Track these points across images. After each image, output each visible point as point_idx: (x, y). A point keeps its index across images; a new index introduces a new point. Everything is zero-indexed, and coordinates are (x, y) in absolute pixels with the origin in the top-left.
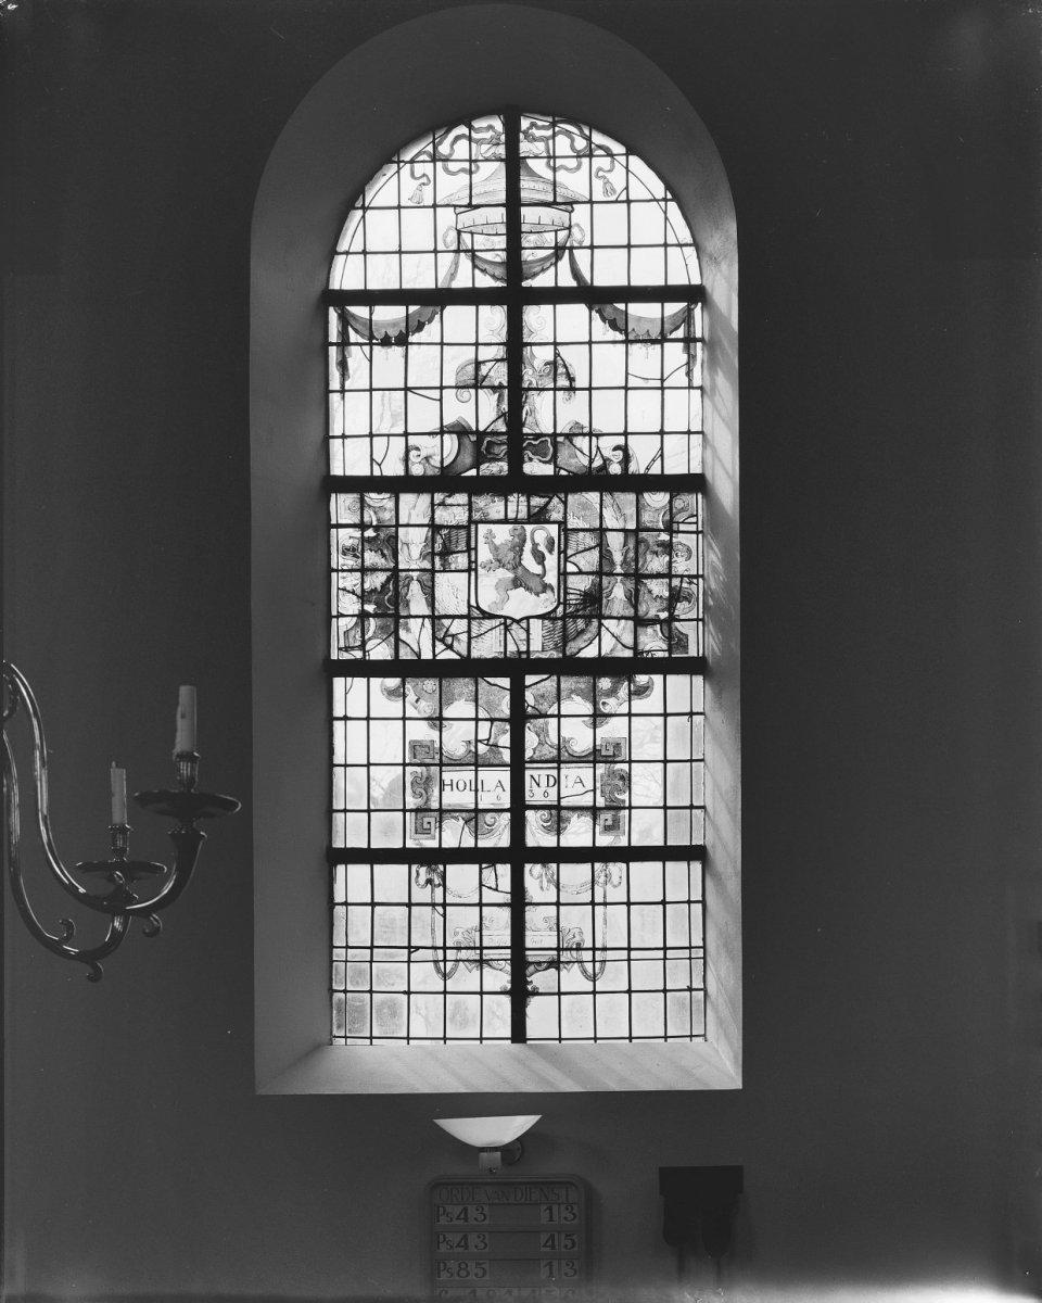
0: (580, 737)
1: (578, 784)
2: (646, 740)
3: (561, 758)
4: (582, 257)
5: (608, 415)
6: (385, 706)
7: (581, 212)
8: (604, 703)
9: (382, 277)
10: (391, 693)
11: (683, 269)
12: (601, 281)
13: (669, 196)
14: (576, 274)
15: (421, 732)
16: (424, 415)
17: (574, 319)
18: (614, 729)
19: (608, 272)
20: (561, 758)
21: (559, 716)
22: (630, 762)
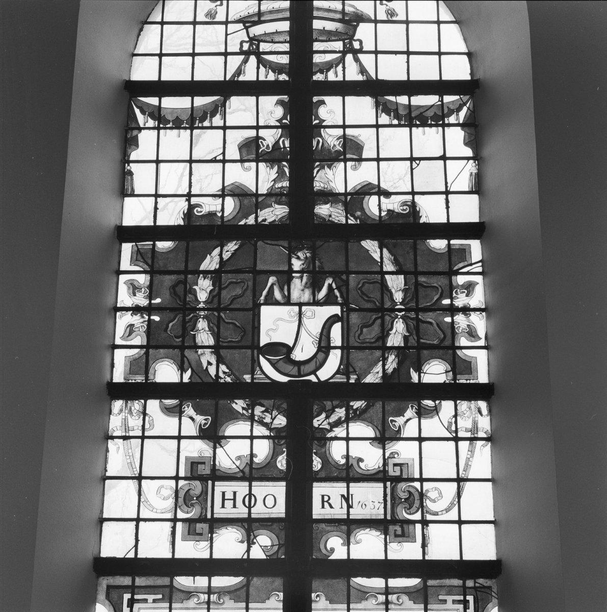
0: (370, 457)
1: (369, 499)
2: (439, 460)
3: (349, 473)
4: (367, 60)
5: (395, 177)
6: (164, 424)
7: (364, 32)
8: (392, 421)
9: (176, 71)
10: (168, 411)
11: (458, 69)
12: (384, 75)
13: (446, 15)
14: (363, 71)
15: (197, 448)
16: (208, 179)
17: (361, 108)
18: (405, 451)
19: (391, 70)
20: (349, 473)
21: (347, 439)
22: (422, 480)
